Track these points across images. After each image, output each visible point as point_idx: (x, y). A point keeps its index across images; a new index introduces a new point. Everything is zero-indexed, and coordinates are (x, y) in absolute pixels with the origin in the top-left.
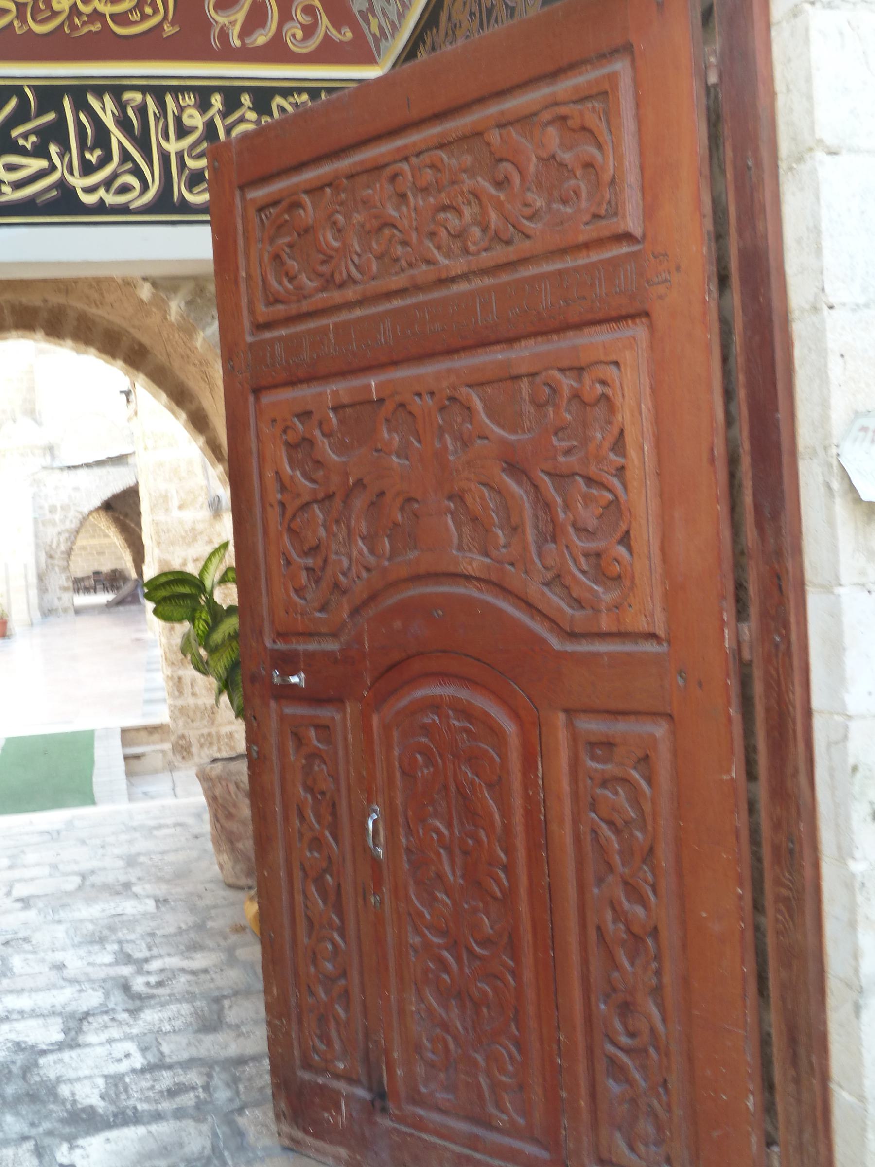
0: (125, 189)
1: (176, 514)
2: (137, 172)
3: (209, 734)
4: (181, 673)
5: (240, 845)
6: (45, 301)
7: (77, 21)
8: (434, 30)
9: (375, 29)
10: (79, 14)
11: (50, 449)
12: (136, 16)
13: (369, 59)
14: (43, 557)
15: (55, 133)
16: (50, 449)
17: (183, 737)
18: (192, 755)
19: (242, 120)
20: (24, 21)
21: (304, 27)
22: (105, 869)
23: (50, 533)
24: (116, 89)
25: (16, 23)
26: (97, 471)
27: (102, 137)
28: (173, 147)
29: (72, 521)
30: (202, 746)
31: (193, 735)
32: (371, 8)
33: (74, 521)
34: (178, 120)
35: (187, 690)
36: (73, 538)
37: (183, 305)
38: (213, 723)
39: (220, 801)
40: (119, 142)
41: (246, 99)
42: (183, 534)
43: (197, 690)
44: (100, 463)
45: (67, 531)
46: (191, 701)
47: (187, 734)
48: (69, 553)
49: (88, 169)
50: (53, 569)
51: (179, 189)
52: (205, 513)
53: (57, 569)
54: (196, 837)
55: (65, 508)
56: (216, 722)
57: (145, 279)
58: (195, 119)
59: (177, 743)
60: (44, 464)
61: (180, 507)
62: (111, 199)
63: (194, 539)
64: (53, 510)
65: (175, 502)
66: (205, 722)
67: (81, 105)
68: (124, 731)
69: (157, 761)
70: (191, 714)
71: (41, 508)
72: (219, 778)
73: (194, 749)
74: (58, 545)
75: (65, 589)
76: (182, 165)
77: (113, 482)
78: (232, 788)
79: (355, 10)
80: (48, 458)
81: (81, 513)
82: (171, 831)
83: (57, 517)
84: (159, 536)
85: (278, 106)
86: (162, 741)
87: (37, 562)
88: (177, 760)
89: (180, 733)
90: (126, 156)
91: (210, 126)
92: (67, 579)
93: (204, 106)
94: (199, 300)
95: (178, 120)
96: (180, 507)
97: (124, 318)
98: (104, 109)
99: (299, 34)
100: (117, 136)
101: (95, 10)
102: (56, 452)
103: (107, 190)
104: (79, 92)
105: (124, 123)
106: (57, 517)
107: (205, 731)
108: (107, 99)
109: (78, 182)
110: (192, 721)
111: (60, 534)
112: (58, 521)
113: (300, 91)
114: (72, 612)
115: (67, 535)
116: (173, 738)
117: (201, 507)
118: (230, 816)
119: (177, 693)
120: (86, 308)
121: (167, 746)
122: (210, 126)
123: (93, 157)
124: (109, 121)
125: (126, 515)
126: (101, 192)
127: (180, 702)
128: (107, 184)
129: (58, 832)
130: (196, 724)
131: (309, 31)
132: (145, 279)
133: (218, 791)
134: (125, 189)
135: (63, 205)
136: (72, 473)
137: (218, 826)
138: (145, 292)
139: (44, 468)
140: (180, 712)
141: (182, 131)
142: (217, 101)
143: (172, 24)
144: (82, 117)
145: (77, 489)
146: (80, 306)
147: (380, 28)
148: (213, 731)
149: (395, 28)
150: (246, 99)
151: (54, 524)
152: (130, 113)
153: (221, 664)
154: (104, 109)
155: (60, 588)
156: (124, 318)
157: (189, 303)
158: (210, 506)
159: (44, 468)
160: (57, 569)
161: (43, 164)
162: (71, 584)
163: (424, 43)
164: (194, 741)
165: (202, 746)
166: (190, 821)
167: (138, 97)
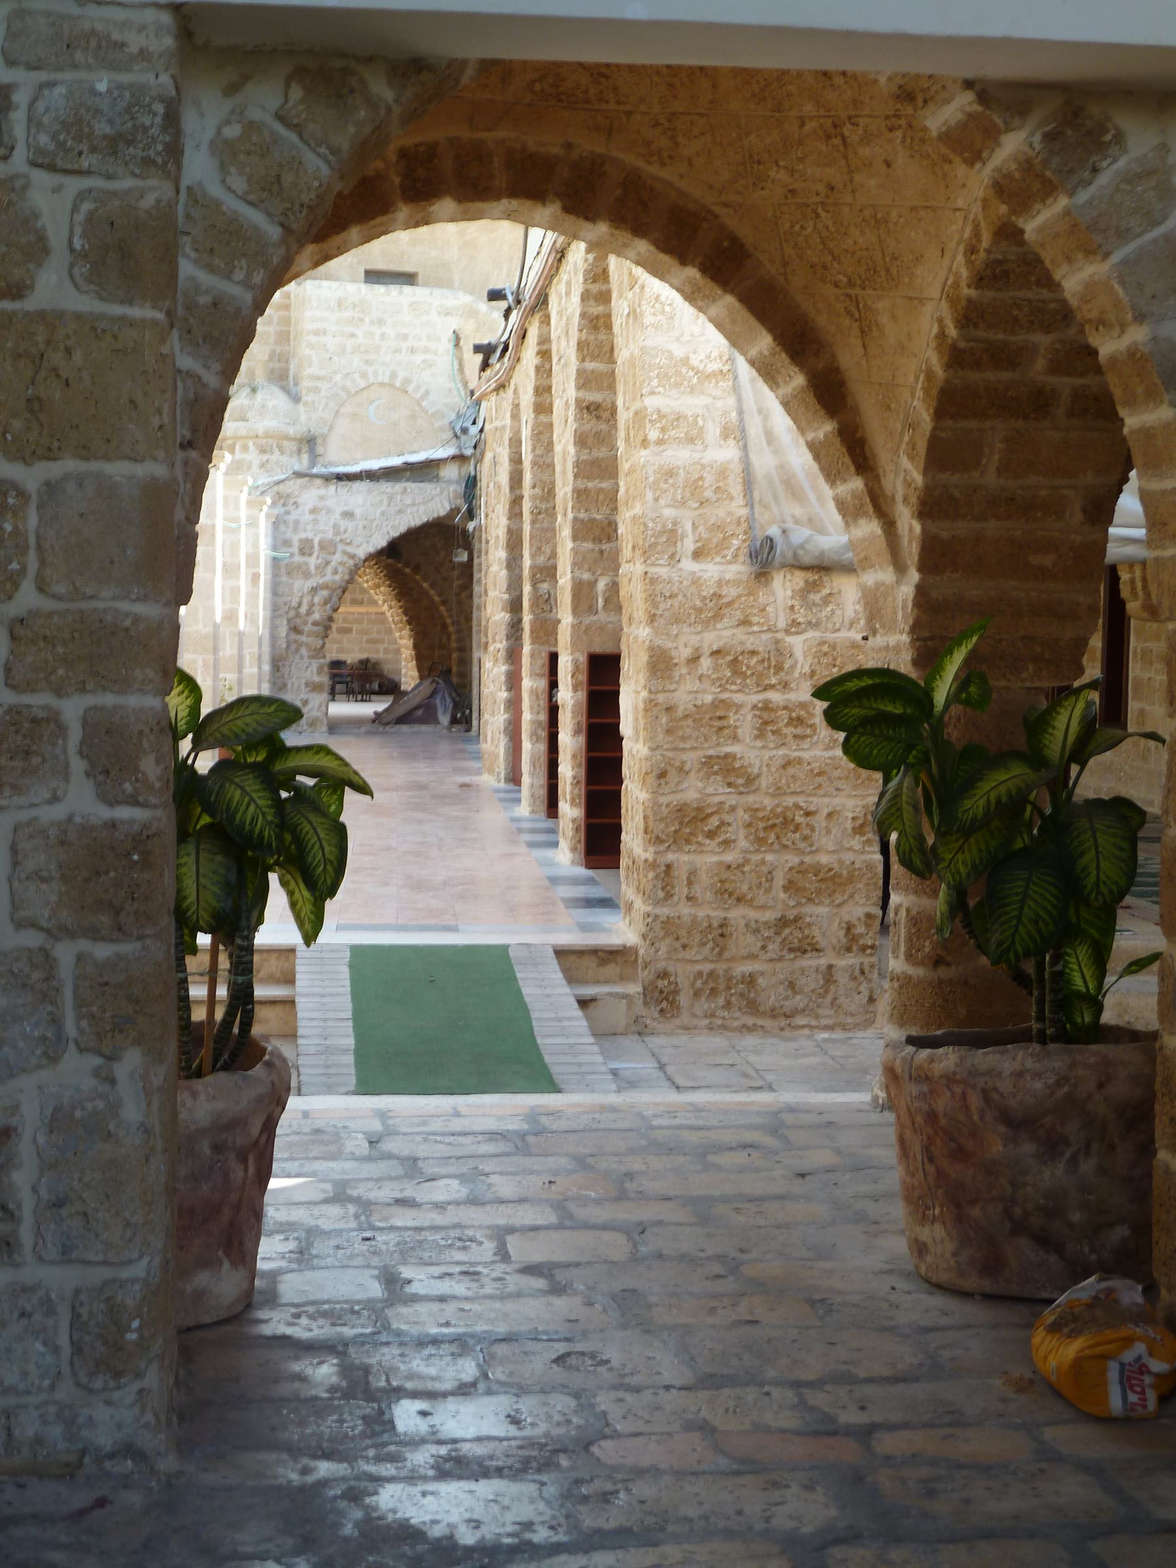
1: (688, 565)
3: (711, 974)
4: (671, 857)
5: (976, 1212)
6: (569, 146)
11: (310, 443)
14: (283, 631)
16: (310, 443)
17: (664, 975)
18: (678, 1008)
22: (660, 1223)
23: (301, 586)
26: (386, 487)
29: (336, 572)
30: (697, 994)
31: (683, 974)
33: (340, 569)
35: (681, 890)
36: (335, 599)
37: (1037, 139)
38: (720, 954)
39: (943, 1122)
42: (698, 603)
43: (697, 891)
44: (390, 474)
45: (325, 587)
46: (686, 910)
47: (671, 969)
48: (326, 625)
50: (297, 650)
52: (739, 570)
53: (304, 651)
54: (803, 1176)
55: (327, 547)
56: (727, 955)
57: (969, 84)
59: (652, 983)
60: (297, 467)
61: (697, 555)
63: (718, 616)
64: (306, 548)
65: (689, 545)
66: (706, 951)
68: (561, 953)
69: (619, 1016)
70: (683, 933)
71: (287, 543)
72: (950, 1079)
73: (683, 999)
74: (309, 612)
75: (315, 688)
77: (425, 504)
78: (975, 1101)
80: (305, 457)
81: (352, 556)
82: (741, 1158)
83: (313, 561)
84: (655, 605)
86: (623, 979)
87: (274, 638)
88: (650, 1015)
89: (661, 965)
92: (320, 670)
94: (1069, 132)
96: (697, 555)
97: (711, 187)
102: (320, 450)
106: (313, 561)
107: (707, 967)
110: (684, 947)
111: (314, 590)
112: (312, 567)
114: (325, 728)
115: (325, 593)
116: (645, 975)
117: (735, 556)
118: (960, 1154)
119: (661, 894)
120: (641, 164)
121: (634, 989)
125: (417, 569)
127: (664, 911)
129: (522, 1136)
130: (688, 954)
132: (969, 84)
133: (942, 1104)
136: (344, 488)
137: (931, 1169)
139: (298, 475)
140: (662, 929)
145: (348, 515)
146: (630, 159)
148: (721, 967)
151: (307, 575)
153: (962, 859)
155: (307, 685)
156: (711, 187)
157: (1049, 137)
158: (753, 555)
159: (298, 475)
160: (304, 651)
162: (325, 679)
164: (683, 983)
165: (697, 994)
166: (769, 1141)
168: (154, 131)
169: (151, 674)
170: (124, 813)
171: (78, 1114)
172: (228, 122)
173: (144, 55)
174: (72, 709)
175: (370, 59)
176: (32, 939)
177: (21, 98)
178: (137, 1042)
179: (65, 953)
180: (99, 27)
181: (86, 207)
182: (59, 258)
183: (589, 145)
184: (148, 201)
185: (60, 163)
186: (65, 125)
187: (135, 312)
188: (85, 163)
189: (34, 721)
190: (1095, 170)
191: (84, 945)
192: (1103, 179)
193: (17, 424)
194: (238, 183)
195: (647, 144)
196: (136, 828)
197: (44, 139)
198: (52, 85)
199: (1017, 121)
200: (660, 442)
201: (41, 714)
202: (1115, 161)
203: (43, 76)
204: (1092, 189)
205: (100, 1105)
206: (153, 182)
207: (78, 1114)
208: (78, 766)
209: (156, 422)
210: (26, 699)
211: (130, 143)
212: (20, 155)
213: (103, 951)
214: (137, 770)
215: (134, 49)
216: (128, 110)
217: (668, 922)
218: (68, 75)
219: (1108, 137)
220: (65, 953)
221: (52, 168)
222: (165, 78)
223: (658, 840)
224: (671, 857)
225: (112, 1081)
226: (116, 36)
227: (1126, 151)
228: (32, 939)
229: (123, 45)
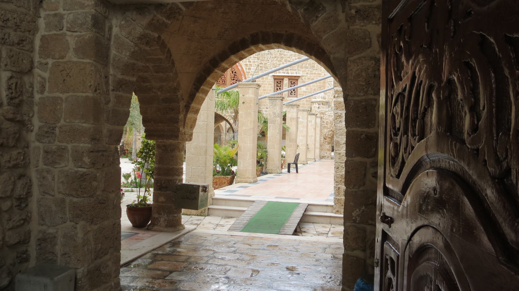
6: (286, 31)
14: (322, 139)
151: (328, 128)
168: (89, 21)
169: (87, 139)
170: (80, 169)
171: (69, 235)
172: (122, 20)
173: (88, 6)
174: (70, 146)
175: (150, 5)
176: (61, 196)
177: (66, 17)
178: (83, 220)
179: (68, 199)
181: (76, 38)
182: (71, 50)
184: (87, 37)
185: (71, 30)
187: (85, 61)
188: (76, 30)
189: (63, 149)
190: (317, 17)
191: (71, 198)
192: (320, 19)
193: (61, 85)
194: (124, 33)
196: (82, 173)
197: (68, 25)
198: (70, 14)
200: (337, 97)
201: (63, 147)
202: (322, 14)
203: (69, 12)
204: (317, 21)
205: (73, 233)
206: (88, 33)
207: (69, 235)
208: (70, 159)
209: (89, 84)
210: (61, 144)
211: (84, 24)
212: (65, 29)
213: (75, 200)
214: (82, 160)
215: (86, 5)
217: (338, 200)
218: (74, 11)
220: (68, 199)
221: (70, 31)
222: (93, 10)
223: (337, 182)
224: (339, 186)
225: (76, 228)
226: (83, 2)
227: (325, 12)
228: (61, 196)
229: (84, 4)
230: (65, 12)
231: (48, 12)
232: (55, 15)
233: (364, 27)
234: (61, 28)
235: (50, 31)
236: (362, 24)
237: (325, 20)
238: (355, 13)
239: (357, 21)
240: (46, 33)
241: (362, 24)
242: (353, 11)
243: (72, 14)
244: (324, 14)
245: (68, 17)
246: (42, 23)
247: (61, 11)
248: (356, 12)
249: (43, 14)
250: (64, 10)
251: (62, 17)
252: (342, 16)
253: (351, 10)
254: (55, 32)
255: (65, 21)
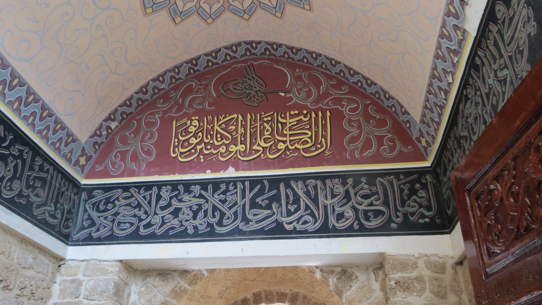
0: (305, 222)
2: (312, 215)
6: (291, 290)
7: (287, 152)
8: (455, 128)
9: (424, 144)
10: (289, 150)
12: (314, 149)
13: (424, 159)
15: (277, 198)
19: (362, 189)
20: (266, 154)
21: (390, 147)
24: (304, 178)
25: (262, 155)
27: (297, 200)
28: (329, 202)
32: (422, 135)
34: (332, 190)
40: (304, 200)
41: (364, 180)
49: (289, 213)
51: (332, 220)
58: (340, 189)
62: (299, 227)
67: (288, 186)
76: (334, 210)
79: (414, 138)
85: (379, 181)
90: (307, 207)
91: (347, 192)
93: (344, 184)
95: (332, 190)
98: (297, 186)
99: (388, 151)
100: (303, 198)
101: (296, 148)
103: (297, 223)
104: (287, 180)
105: (307, 193)
108: (300, 184)
109: (285, 220)
113: (390, 174)
122: (347, 192)
123: (292, 208)
124: (300, 192)
126: (295, 224)
128: (298, 220)
131: (392, 149)
134: (305, 222)
135: (278, 232)
138: (318, 275)
141: (333, 196)
142: (350, 181)
143: (329, 151)
144: (287, 191)
147: (427, 142)
149: (434, 138)
150: (364, 180)
152: (309, 188)
154: (297, 186)
161: (269, 211)
163: (450, 137)
167: (313, 181)
168: (111, 289)
172: (142, 287)
173: (112, 272)
175: (174, 271)
177: (84, 283)
180: (103, 266)
183: (296, 290)
186: (92, 289)
188: (94, 298)
192: (353, 288)
194: (142, 301)
195: (308, 289)
198: (91, 280)
199: (331, 276)
202: (356, 283)
204: (351, 291)
206: (109, 301)
215: (110, 271)
216: (106, 285)
219: (353, 278)
221: (87, 299)
222: (116, 277)
226: (106, 268)
229: (107, 270)
230: (85, 278)
231: (65, 278)
232: (73, 281)
233: (406, 300)
234: (78, 296)
235: (64, 298)
236: (404, 296)
237: (359, 290)
238: (394, 285)
239: (398, 292)
240: (59, 301)
241: (404, 296)
242: (393, 283)
243: (93, 281)
244: (358, 284)
245: (88, 284)
246: (56, 289)
247: (80, 276)
248: (396, 283)
249: (59, 279)
250: (84, 276)
251: (80, 283)
252: (376, 286)
253: (390, 281)
254: (69, 300)
255: (83, 288)
